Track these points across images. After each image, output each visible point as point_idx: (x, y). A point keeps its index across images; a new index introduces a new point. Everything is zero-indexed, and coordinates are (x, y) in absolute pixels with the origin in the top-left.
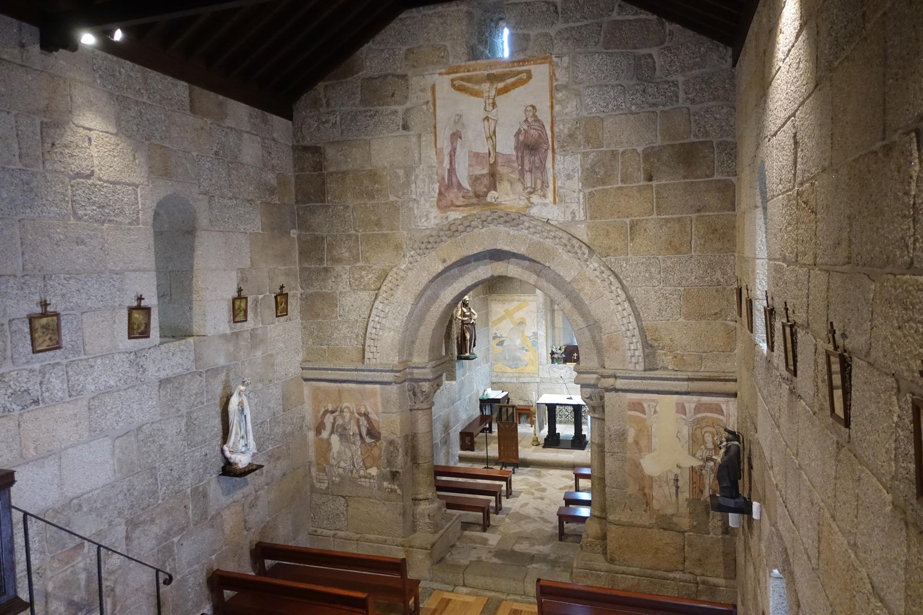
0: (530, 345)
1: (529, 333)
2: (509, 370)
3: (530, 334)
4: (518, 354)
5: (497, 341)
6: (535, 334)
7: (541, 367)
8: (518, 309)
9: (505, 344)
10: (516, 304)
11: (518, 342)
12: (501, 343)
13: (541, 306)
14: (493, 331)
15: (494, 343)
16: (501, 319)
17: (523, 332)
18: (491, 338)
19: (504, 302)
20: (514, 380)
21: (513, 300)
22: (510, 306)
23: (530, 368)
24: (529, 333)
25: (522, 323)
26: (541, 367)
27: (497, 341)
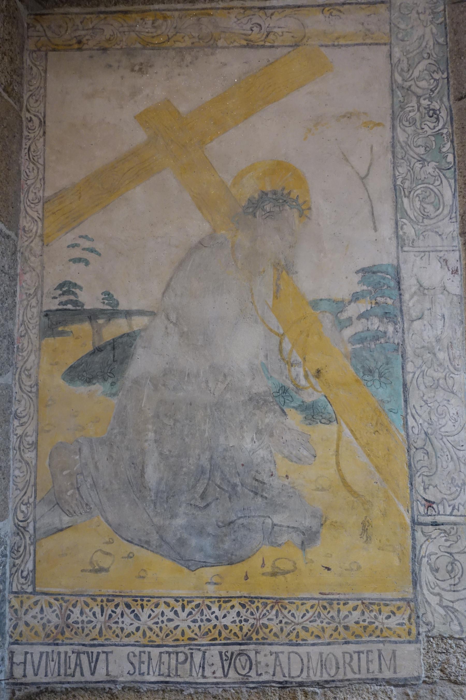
0: (340, 368)
1: (329, 272)
2: (165, 577)
3: (344, 285)
4: (247, 445)
5: (79, 341)
6: (383, 284)
7: (432, 547)
8: (254, 96)
9: (142, 363)
10: (232, 65)
11: (244, 349)
12: (106, 362)
13: (423, 76)
14: (49, 265)
15: (45, 362)
16: (106, 185)
17: (284, 268)
18: (27, 316)
19: (138, 56)
20: (210, 668)
21: (209, 43)
22: (188, 86)
23: (346, 561)
24: (329, 272)
25: (277, 200)
26: (432, 547)
27: (79, 341)
